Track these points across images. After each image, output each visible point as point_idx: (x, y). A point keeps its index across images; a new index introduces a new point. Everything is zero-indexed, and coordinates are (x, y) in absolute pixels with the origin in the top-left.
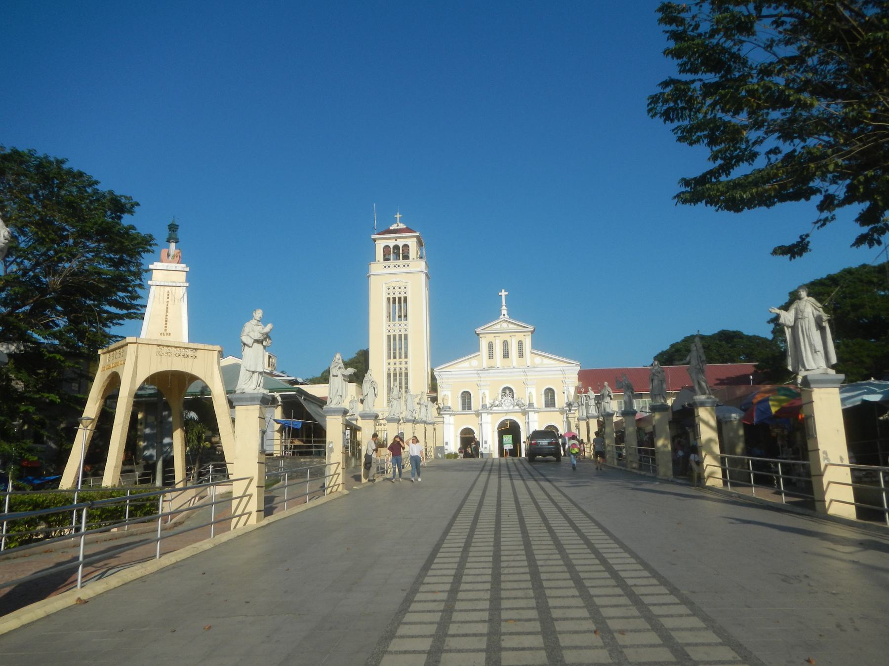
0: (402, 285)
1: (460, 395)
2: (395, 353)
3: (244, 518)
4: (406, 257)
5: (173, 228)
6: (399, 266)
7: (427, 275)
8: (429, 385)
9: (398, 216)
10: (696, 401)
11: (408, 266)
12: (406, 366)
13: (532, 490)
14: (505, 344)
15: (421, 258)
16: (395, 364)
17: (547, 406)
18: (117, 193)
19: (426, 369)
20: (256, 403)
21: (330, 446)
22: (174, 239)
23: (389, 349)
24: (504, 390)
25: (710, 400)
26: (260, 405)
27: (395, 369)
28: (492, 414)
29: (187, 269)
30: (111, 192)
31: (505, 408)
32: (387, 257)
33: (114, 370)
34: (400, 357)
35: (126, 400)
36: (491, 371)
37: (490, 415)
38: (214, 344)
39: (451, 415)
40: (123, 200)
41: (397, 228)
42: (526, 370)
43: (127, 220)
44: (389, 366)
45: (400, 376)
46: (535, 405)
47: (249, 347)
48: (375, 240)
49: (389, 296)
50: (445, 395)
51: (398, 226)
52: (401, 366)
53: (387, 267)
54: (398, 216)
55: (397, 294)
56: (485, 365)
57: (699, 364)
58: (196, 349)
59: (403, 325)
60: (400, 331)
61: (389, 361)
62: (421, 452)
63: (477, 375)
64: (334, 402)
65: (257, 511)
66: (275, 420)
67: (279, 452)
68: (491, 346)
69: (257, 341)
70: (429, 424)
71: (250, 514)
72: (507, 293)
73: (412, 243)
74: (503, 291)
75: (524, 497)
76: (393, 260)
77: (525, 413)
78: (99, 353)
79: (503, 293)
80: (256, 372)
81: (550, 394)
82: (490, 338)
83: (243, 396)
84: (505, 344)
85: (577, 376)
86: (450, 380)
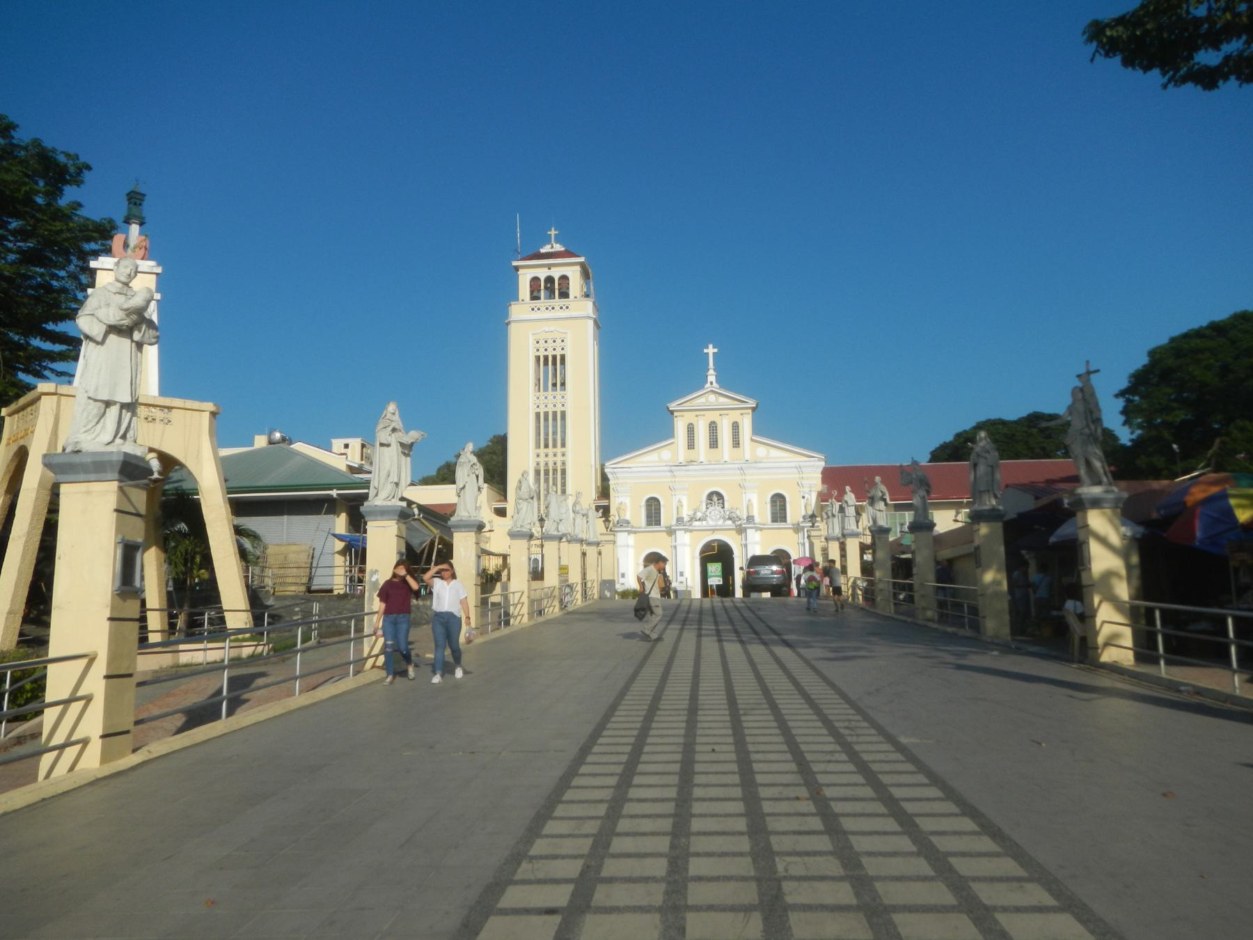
0: (558, 337)
1: (643, 503)
2: (546, 440)
3: (70, 753)
4: (564, 295)
5: (135, 199)
6: (553, 308)
7: (595, 322)
8: (597, 487)
9: (553, 232)
10: (1083, 496)
11: (567, 308)
13: (759, 667)
14: (713, 427)
15: (587, 296)
16: (547, 455)
17: (774, 520)
18: (48, 143)
19: (593, 463)
20: (109, 476)
21: (374, 579)
22: (136, 217)
23: (538, 434)
24: (710, 496)
25: (1111, 496)
26: (120, 481)
27: (547, 464)
28: (691, 531)
29: (159, 270)
30: (37, 143)
31: (711, 523)
33: (22, 442)
34: (555, 446)
35: (33, 495)
36: (691, 467)
37: (688, 534)
38: (202, 400)
39: (629, 532)
40: (62, 159)
41: (551, 250)
42: (743, 465)
43: (70, 194)
44: (538, 460)
45: (554, 474)
46: (757, 520)
47: (98, 343)
48: (517, 268)
49: (538, 354)
50: (621, 503)
51: (552, 247)
52: (555, 459)
53: (536, 309)
54: (553, 232)
55: (550, 349)
56: (681, 459)
57: (1088, 426)
58: (170, 408)
59: (559, 397)
60: (555, 406)
61: (538, 451)
62: (464, 602)
64: (383, 495)
65: (103, 737)
66: (335, 536)
67: (342, 587)
68: (691, 429)
69: (113, 329)
70: (589, 544)
71: (85, 742)
72: (716, 350)
73: (574, 274)
74: (711, 346)
75: (747, 691)
76: (545, 299)
77: (741, 530)
78: (3, 414)
79: (711, 350)
80: (115, 403)
81: (779, 503)
83: (76, 459)
84: (713, 427)
85: (821, 476)
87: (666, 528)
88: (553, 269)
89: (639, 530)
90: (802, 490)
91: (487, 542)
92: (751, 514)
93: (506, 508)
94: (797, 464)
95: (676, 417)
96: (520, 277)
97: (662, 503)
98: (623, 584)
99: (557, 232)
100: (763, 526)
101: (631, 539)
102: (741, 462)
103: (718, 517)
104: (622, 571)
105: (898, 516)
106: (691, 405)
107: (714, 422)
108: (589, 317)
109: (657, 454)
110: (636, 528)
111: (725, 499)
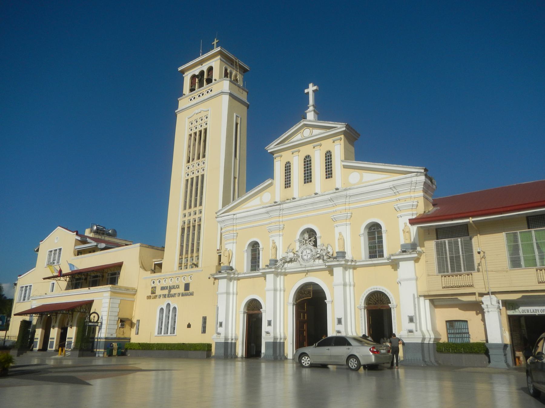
4: (209, 81)
7: (231, 95)
9: (216, 41)
11: (211, 91)
12: (200, 216)
14: (308, 162)
27: (190, 222)
28: (285, 274)
32: (193, 88)
34: (195, 206)
36: (285, 206)
39: (230, 279)
44: (184, 219)
56: (278, 199)
59: (201, 164)
63: (267, 216)
68: (288, 168)
72: (315, 88)
73: (216, 63)
82: (286, 156)
84: (308, 162)
86: (235, 228)
88: (204, 65)
89: (239, 276)
91: (135, 294)
92: (342, 250)
93: (162, 263)
94: (390, 184)
95: (275, 159)
96: (185, 78)
97: (261, 246)
98: (219, 334)
99: (218, 41)
100: (353, 263)
101: (234, 286)
102: (332, 191)
103: (309, 256)
104: (220, 320)
105: (533, 233)
106: (289, 142)
107: (309, 156)
108: (223, 93)
109: (259, 198)
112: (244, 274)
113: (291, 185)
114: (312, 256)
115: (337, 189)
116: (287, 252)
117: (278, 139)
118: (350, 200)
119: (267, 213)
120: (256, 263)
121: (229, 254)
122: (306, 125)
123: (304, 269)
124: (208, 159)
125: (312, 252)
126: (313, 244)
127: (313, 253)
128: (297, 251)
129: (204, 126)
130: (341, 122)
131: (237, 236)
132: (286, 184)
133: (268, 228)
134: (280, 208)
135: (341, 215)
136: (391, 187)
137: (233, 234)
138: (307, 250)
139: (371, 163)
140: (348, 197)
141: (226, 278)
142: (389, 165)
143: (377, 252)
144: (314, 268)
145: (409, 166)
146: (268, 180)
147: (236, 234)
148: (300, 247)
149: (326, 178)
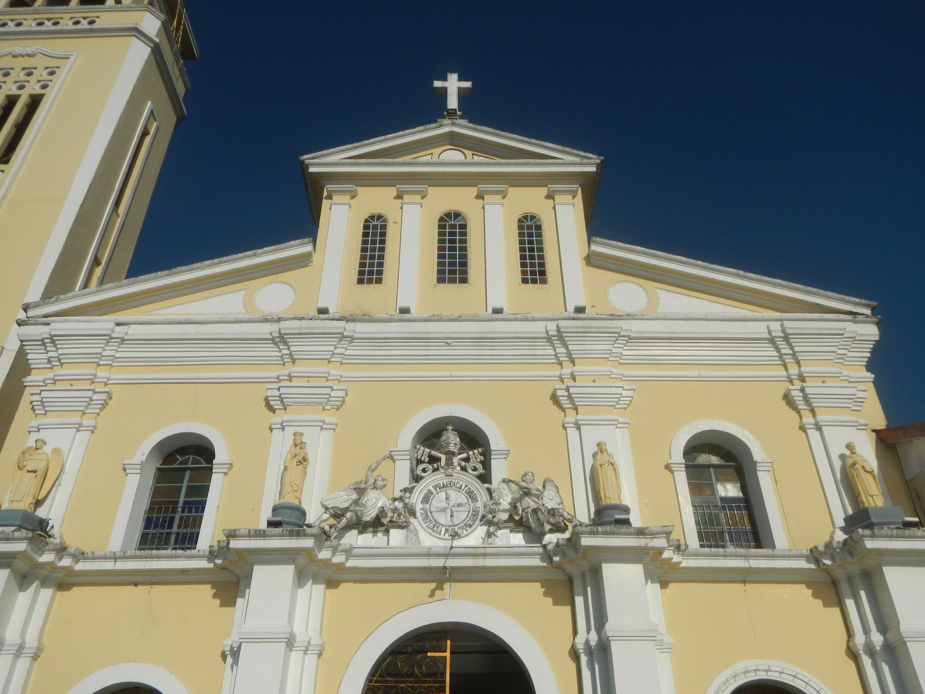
7: (156, 51)
31: (428, 540)
36: (360, 329)
37: (314, 592)
42: (562, 323)
63: (272, 351)
72: (467, 84)
74: (453, 78)
79: (453, 85)
86: (102, 373)
87: (212, 555)
89: (80, 566)
90: (808, 419)
95: (330, 197)
97: (221, 456)
100: (676, 558)
103: (461, 516)
107: (457, 215)
108: (136, 32)
110: (62, 550)
111: (493, 447)
112: (115, 558)
113: (386, 277)
114: (475, 514)
115: (580, 310)
116: (363, 486)
117: (355, 145)
118: (625, 353)
119: (281, 339)
120: (170, 527)
121: (48, 469)
122: (454, 140)
123: (438, 563)
124: (16, 175)
125: (474, 499)
126: (481, 470)
127: (479, 504)
128: (405, 490)
129: (33, 88)
130: (585, 151)
131: (104, 405)
132: (361, 273)
133: (276, 393)
134: (345, 329)
135: (595, 390)
136: (774, 334)
137: (90, 394)
138: (453, 494)
139: (699, 262)
140: (622, 341)
141: (8, 567)
142: (758, 277)
143: (727, 535)
144: (490, 562)
145: (825, 289)
146: (297, 242)
147: (104, 396)
148: (417, 479)
149: (525, 281)
